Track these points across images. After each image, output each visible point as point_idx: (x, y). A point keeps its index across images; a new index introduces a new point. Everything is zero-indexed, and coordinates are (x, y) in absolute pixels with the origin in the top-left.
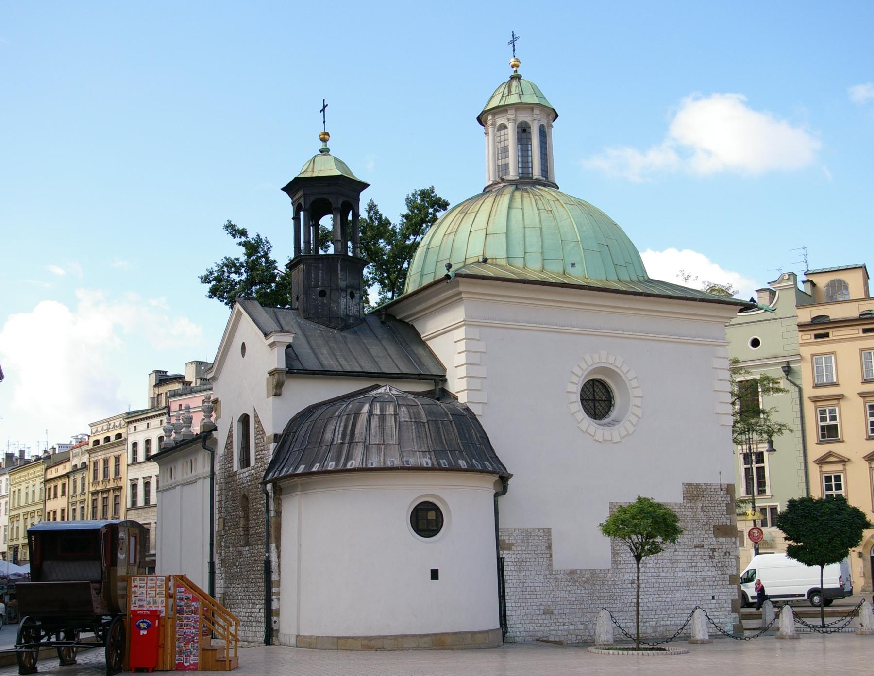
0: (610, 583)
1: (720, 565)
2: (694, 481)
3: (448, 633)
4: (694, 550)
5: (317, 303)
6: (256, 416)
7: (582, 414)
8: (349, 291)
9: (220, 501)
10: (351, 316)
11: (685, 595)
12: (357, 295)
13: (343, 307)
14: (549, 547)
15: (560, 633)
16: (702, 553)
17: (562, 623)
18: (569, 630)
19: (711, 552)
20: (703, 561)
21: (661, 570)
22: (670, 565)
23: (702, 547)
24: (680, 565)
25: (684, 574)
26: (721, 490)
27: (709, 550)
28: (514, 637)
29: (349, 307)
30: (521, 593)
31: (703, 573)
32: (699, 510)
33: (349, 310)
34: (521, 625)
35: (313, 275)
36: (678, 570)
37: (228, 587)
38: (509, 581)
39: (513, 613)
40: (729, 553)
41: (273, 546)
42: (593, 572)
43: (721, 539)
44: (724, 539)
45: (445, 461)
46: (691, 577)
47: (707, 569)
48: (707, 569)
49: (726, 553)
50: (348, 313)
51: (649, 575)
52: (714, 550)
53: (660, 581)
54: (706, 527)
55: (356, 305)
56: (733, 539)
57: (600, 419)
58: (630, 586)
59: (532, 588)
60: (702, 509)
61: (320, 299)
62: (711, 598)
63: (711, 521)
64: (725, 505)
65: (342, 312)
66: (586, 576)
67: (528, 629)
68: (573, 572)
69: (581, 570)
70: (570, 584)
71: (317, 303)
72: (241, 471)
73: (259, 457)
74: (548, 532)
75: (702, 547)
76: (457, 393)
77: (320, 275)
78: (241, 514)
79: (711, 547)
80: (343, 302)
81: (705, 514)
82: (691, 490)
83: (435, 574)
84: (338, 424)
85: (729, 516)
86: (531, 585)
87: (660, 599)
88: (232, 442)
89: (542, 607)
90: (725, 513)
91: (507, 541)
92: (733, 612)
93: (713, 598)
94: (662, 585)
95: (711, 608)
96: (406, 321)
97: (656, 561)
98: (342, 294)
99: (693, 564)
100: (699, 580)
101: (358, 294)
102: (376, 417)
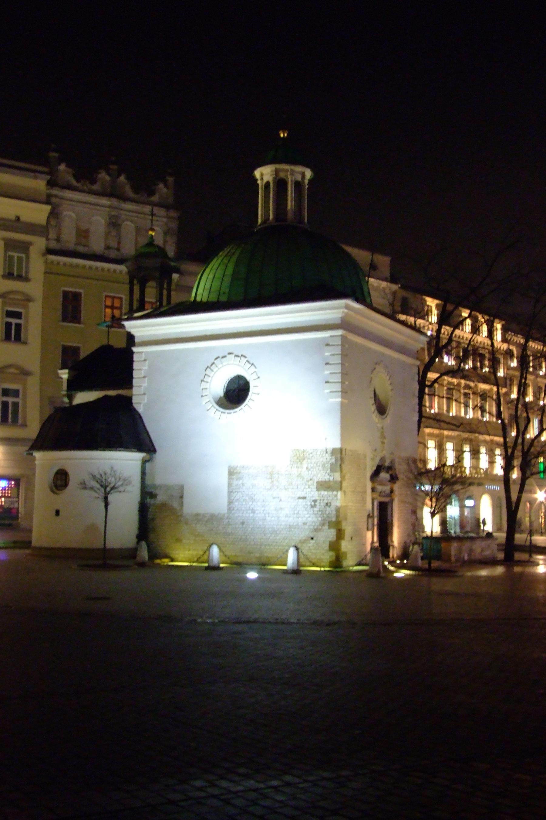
4: (297, 500)
14: (181, 497)
19: (313, 503)
23: (305, 498)
25: (287, 519)
26: (327, 453)
27: (311, 501)
40: (330, 503)
43: (323, 492)
44: (326, 493)
48: (307, 516)
49: (327, 504)
52: (315, 501)
53: (265, 523)
54: (310, 483)
56: (335, 493)
58: (241, 526)
60: (307, 468)
62: (310, 539)
64: (329, 465)
68: (198, 515)
74: (182, 488)
75: (305, 498)
79: (314, 498)
81: (310, 472)
83: (58, 513)
85: (332, 474)
87: (264, 537)
90: (329, 471)
91: (154, 493)
93: (312, 538)
95: (310, 547)
97: (263, 509)
100: (300, 524)
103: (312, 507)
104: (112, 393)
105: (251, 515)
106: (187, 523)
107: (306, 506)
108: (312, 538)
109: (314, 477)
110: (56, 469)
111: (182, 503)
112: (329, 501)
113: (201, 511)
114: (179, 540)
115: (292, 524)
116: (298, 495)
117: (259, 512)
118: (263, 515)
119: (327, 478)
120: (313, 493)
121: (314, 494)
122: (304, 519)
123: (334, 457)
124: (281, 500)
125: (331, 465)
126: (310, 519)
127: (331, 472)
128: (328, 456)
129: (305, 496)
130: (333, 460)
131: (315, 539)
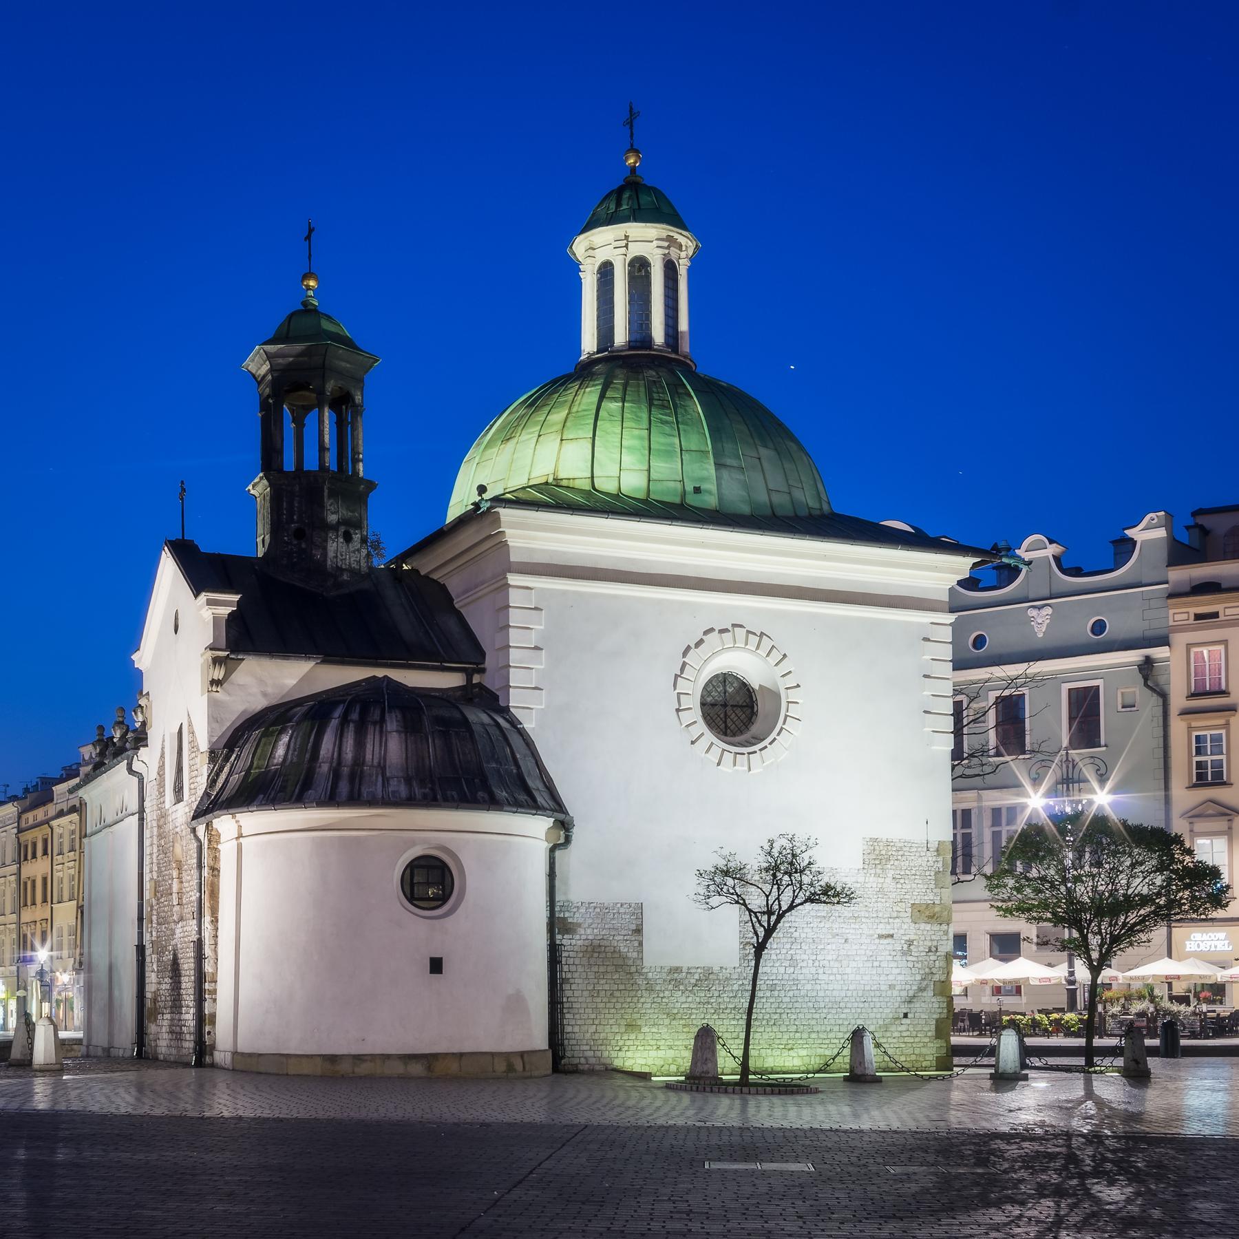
0: (736, 987)
1: (920, 966)
2: (884, 835)
3: (453, 1054)
4: (877, 941)
5: (292, 549)
6: (190, 725)
7: (701, 727)
8: (342, 529)
9: (151, 854)
10: (345, 570)
11: (859, 1010)
12: (357, 537)
13: (331, 554)
14: (639, 931)
15: (650, 1062)
16: (890, 947)
17: (655, 1047)
18: (664, 1059)
19: (905, 947)
20: (890, 958)
21: (821, 971)
22: (837, 964)
23: (892, 936)
24: (853, 964)
27: (903, 942)
28: (577, 1065)
29: (342, 555)
30: (589, 1000)
31: (891, 977)
32: (889, 880)
33: (342, 560)
34: (588, 1047)
35: (285, 504)
36: (848, 970)
37: (159, 983)
38: (571, 981)
39: (576, 1029)
41: (207, 919)
42: (708, 973)
43: (923, 926)
44: (928, 927)
45: (454, 793)
46: (871, 982)
47: (898, 971)
48: (898, 971)
49: (930, 951)
50: (339, 565)
51: (801, 977)
52: (910, 943)
53: (818, 987)
55: (354, 552)
57: (734, 735)
58: (768, 994)
59: (608, 993)
61: (295, 542)
62: (902, 1015)
63: (907, 897)
64: (933, 873)
65: (329, 563)
66: (697, 977)
67: (599, 1054)
68: (677, 970)
69: (689, 969)
70: (671, 987)
71: (292, 549)
72: (175, 808)
73: (192, 786)
76: (497, 690)
77: (296, 505)
78: (175, 874)
79: (907, 938)
80: (332, 547)
81: (899, 886)
82: (877, 848)
83: (436, 966)
84: (295, 735)
85: (938, 890)
86: (607, 987)
87: (817, 1016)
88: (164, 763)
89: (623, 1022)
90: (932, 886)
92: (937, 1037)
93: (906, 1016)
94: (821, 994)
96: (435, 576)
97: (814, 957)
98: (331, 535)
99: (876, 964)
101: (359, 536)
102: (352, 725)
103: (904, 953)
104: (380, 673)
105: (792, 970)
106: (650, 989)
107: (894, 953)
108: (906, 1016)
109: (907, 897)
110: (417, 851)
111: (641, 944)
112: (935, 943)
113: (685, 964)
114: (632, 1027)
115: (868, 988)
116: (880, 932)
117: (804, 964)
118: (813, 970)
119: (929, 898)
120: (905, 926)
121: (906, 929)
122: (891, 977)
123: (940, 859)
124: (846, 941)
125: (937, 873)
126: (900, 978)
127: (936, 886)
128: (931, 856)
129: (891, 933)
130: (940, 865)
131: (909, 1015)
